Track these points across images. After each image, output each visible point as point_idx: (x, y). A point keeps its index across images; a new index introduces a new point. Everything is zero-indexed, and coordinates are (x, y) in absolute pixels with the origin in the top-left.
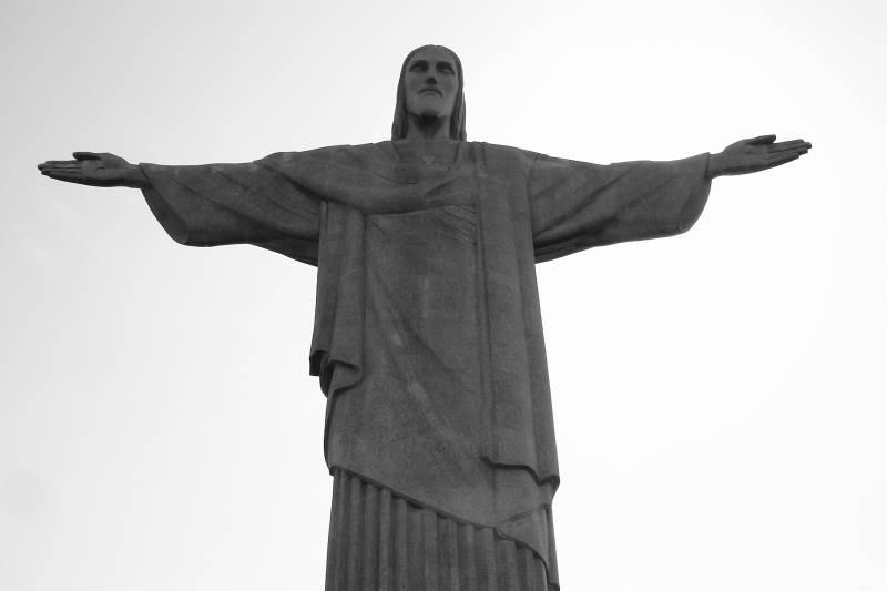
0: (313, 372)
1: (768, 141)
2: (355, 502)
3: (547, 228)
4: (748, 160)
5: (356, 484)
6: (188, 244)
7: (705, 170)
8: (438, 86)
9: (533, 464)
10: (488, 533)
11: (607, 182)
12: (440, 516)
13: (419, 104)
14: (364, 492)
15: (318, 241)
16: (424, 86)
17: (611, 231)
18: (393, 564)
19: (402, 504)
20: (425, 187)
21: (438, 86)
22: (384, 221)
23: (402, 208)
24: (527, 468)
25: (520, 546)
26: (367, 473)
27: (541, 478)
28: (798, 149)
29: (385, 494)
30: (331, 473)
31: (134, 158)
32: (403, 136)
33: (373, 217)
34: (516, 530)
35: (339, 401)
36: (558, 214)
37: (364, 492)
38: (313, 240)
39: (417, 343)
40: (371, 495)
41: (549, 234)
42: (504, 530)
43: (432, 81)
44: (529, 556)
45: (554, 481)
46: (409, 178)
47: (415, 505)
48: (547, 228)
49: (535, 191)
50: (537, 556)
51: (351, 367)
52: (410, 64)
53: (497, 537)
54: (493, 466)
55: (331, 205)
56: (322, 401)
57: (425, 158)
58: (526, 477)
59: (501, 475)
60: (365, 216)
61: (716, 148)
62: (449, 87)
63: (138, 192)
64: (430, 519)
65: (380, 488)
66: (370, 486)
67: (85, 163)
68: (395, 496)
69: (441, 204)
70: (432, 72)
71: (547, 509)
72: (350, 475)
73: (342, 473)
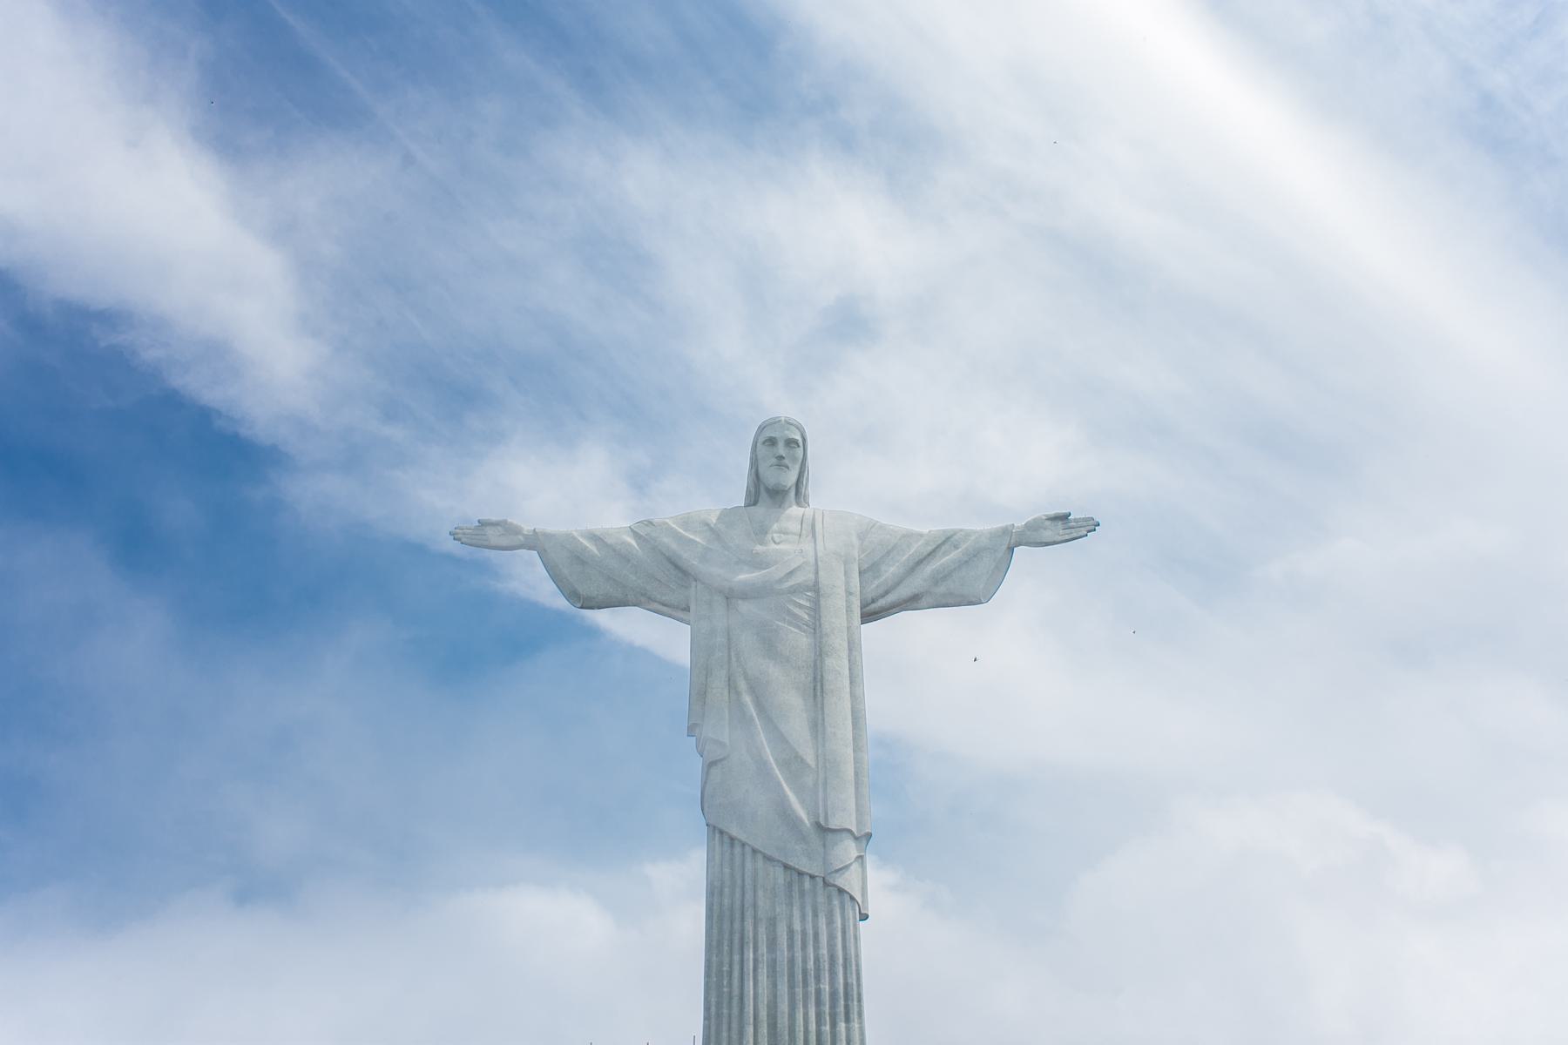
1: (1064, 518)
2: (727, 855)
3: (873, 601)
4: (1047, 535)
5: (726, 839)
7: (1011, 541)
8: (786, 461)
9: (854, 830)
10: (821, 883)
12: (786, 867)
13: (771, 477)
14: (732, 845)
16: (774, 461)
17: (924, 602)
18: (755, 906)
19: (760, 857)
20: (776, 572)
21: (786, 461)
22: (745, 607)
24: (849, 831)
25: (841, 891)
26: (734, 831)
28: (1092, 525)
29: (748, 849)
31: (527, 528)
32: (755, 503)
34: (840, 881)
35: (715, 771)
37: (732, 845)
38: (687, 609)
40: (738, 850)
41: (873, 606)
43: (781, 458)
44: (847, 898)
45: (869, 836)
47: (768, 859)
50: (852, 898)
52: (761, 439)
54: (823, 830)
59: (830, 836)
61: (1020, 524)
62: (794, 459)
64: (780, 870)
65: (743, 845)
67: (490, 531)
68: (754, 851)
70: (781, 450)
71: (861, 858)
72: (721, 832)
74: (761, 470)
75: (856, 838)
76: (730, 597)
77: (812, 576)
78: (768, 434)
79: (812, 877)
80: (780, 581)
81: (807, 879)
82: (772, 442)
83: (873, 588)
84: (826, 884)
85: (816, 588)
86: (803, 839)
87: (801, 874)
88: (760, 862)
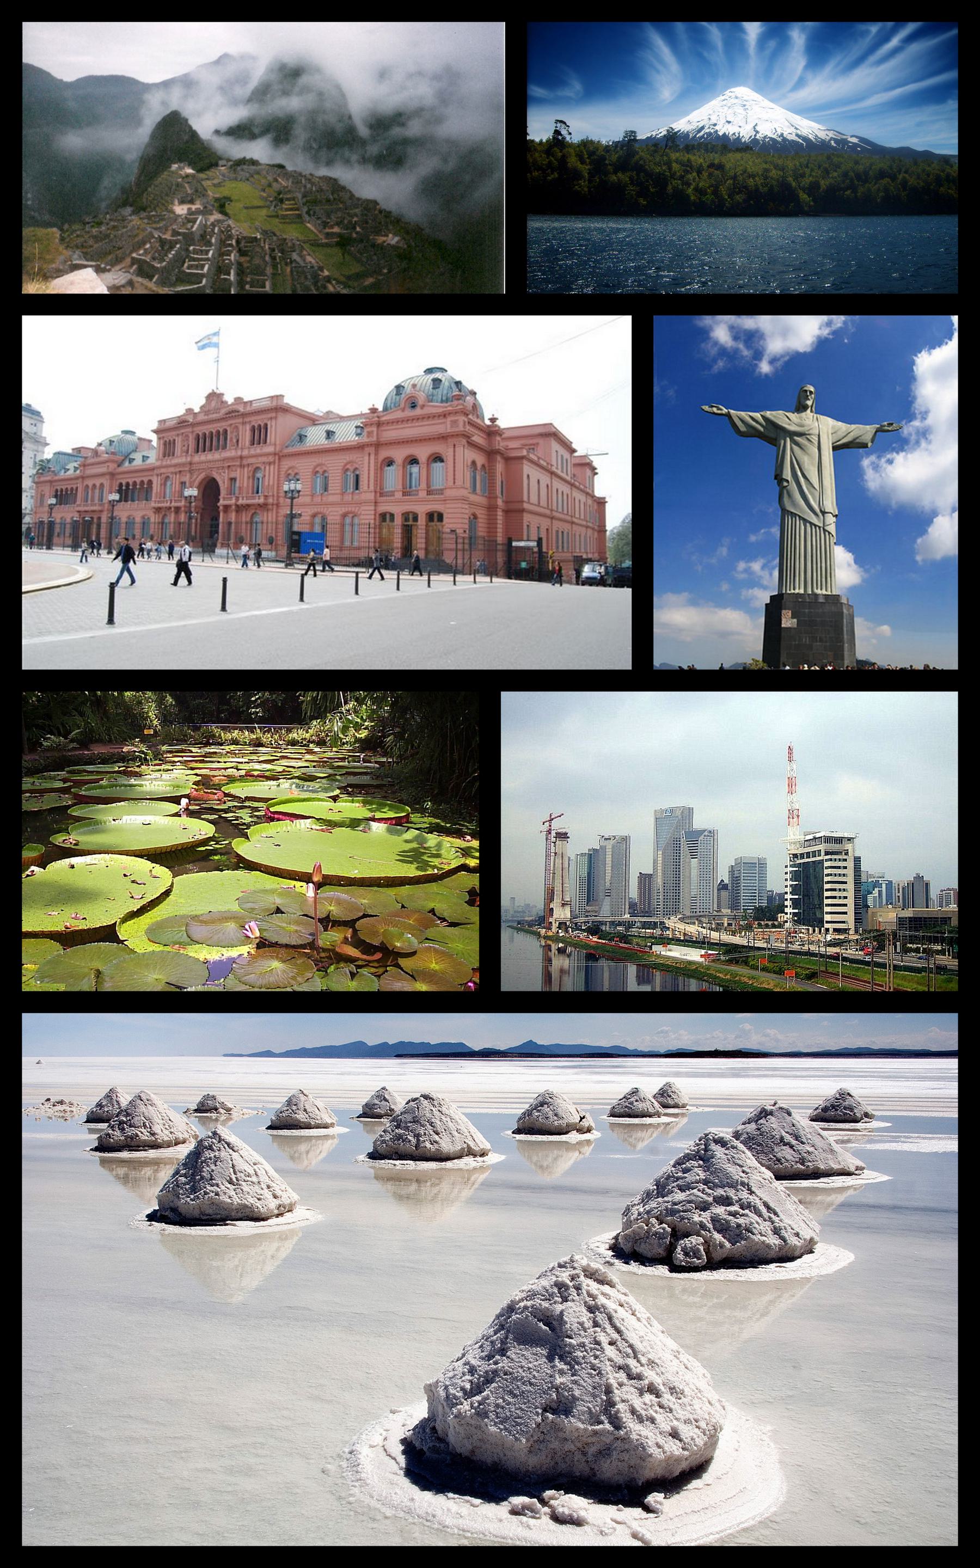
0: (776, 478)
22: (796, 438)
23: (801, 434)
46: (802, 426)
51: (787, 481)
76: (792, 434)
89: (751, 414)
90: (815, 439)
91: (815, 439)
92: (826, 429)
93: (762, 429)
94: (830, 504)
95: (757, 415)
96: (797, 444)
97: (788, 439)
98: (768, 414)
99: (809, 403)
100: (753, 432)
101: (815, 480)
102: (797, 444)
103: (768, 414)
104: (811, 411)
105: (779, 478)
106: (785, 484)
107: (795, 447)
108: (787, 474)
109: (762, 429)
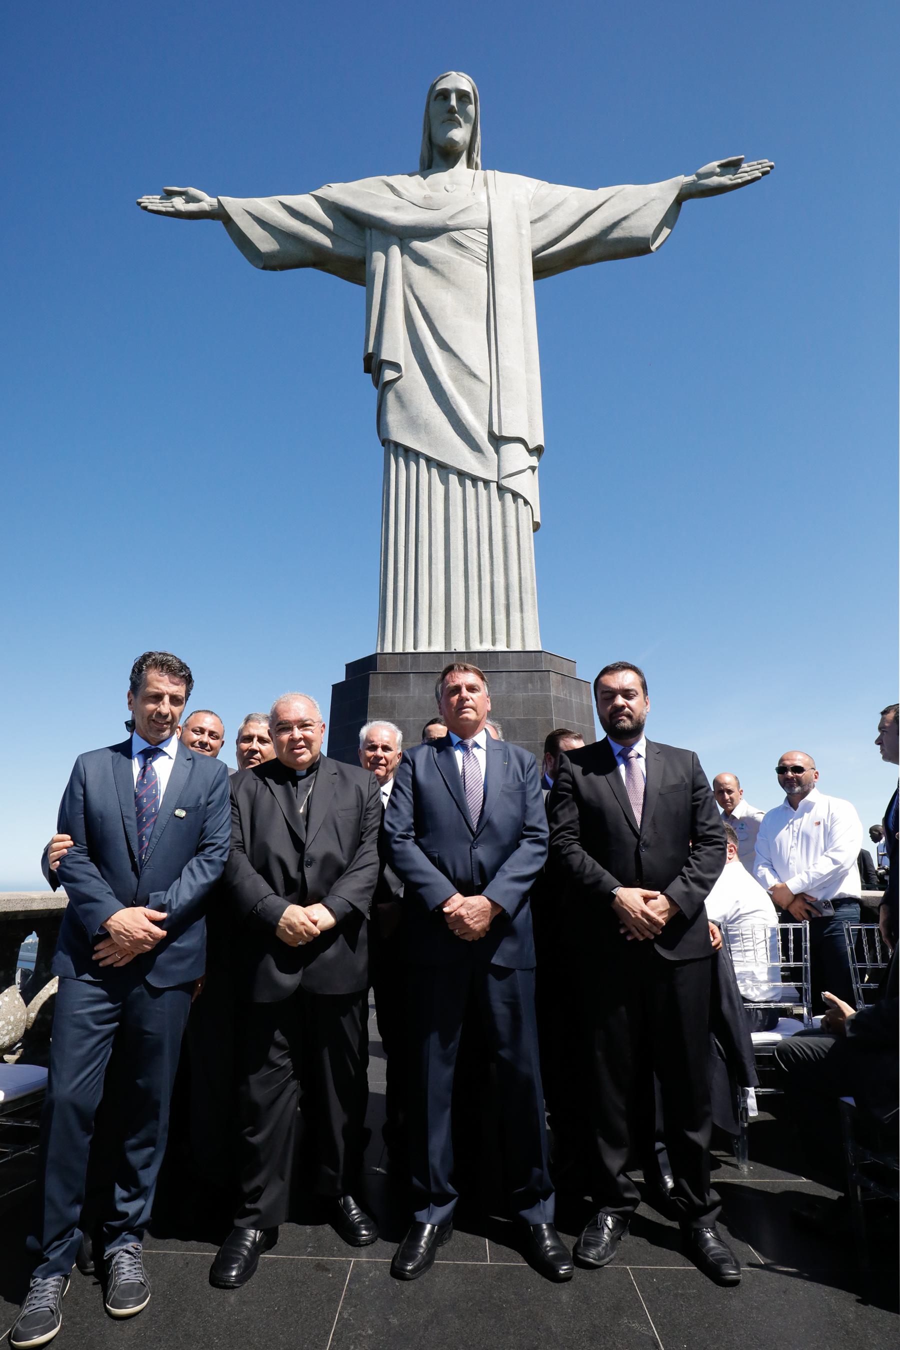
0: (367, 370)
6: (264, 268)
10: (493, 486)
11: (595, 206)
12: (462, 475)
15: (365, 264)
16: (447, 116)
22: (417, 245)
23: (430, 233)
25: (516, 495)
27: (530, 447)
30: (383, 445)
32: (430, 167)
33: (407, 241)
36: (554, 235)
39: (443, 345)
42: (505, 483)
43: (451, 111)
44: (521, 501)
48: (544, 248)
49: (536, 216)
50: (526, 502)
51: (396, 367)
52: (434, 94)
53: (501, 489)
54: (498, 441)
55: (374, 232)
56: (374, 392)
57: (448, 188)
58: (520, 446)
60: (401, 240)
63: (220, 222)
65: (418, 455)
66: (410, 453)
68: (429, 460)
69: (458, 229)
70: (454, 102)
73: (392, 445)
74: (433, 131)
75: (531, 452)
76: (405, 236)
77: (487, 216)
78: (438, 87)
79: (487, 483)
80: (452, 217)
81: (480, 484)
82: (445, 95)
83: (545, 233)
84: (501, 489)
85: (489, 229)
86: (474, 446)
87: (475, 480)
88: (434, 471)
89: (292, 200)
90: (476, 241)
91: (476, 241)
92: (508, 209)
93: (325, 241)
94: (525, 416)
95: (306, 202)
96: (421, 260)
97: (395, 250)
98: (337, 192)
99: (460, 134)
100: (295, 251)
101: (475, 354)
102: (421, 260)
103: (340, 192)
104: (470, 163)
105: (374, 364)
106: (389, 375)
107: (417, 271)
108: (396, 347)
109: (326, 241)
